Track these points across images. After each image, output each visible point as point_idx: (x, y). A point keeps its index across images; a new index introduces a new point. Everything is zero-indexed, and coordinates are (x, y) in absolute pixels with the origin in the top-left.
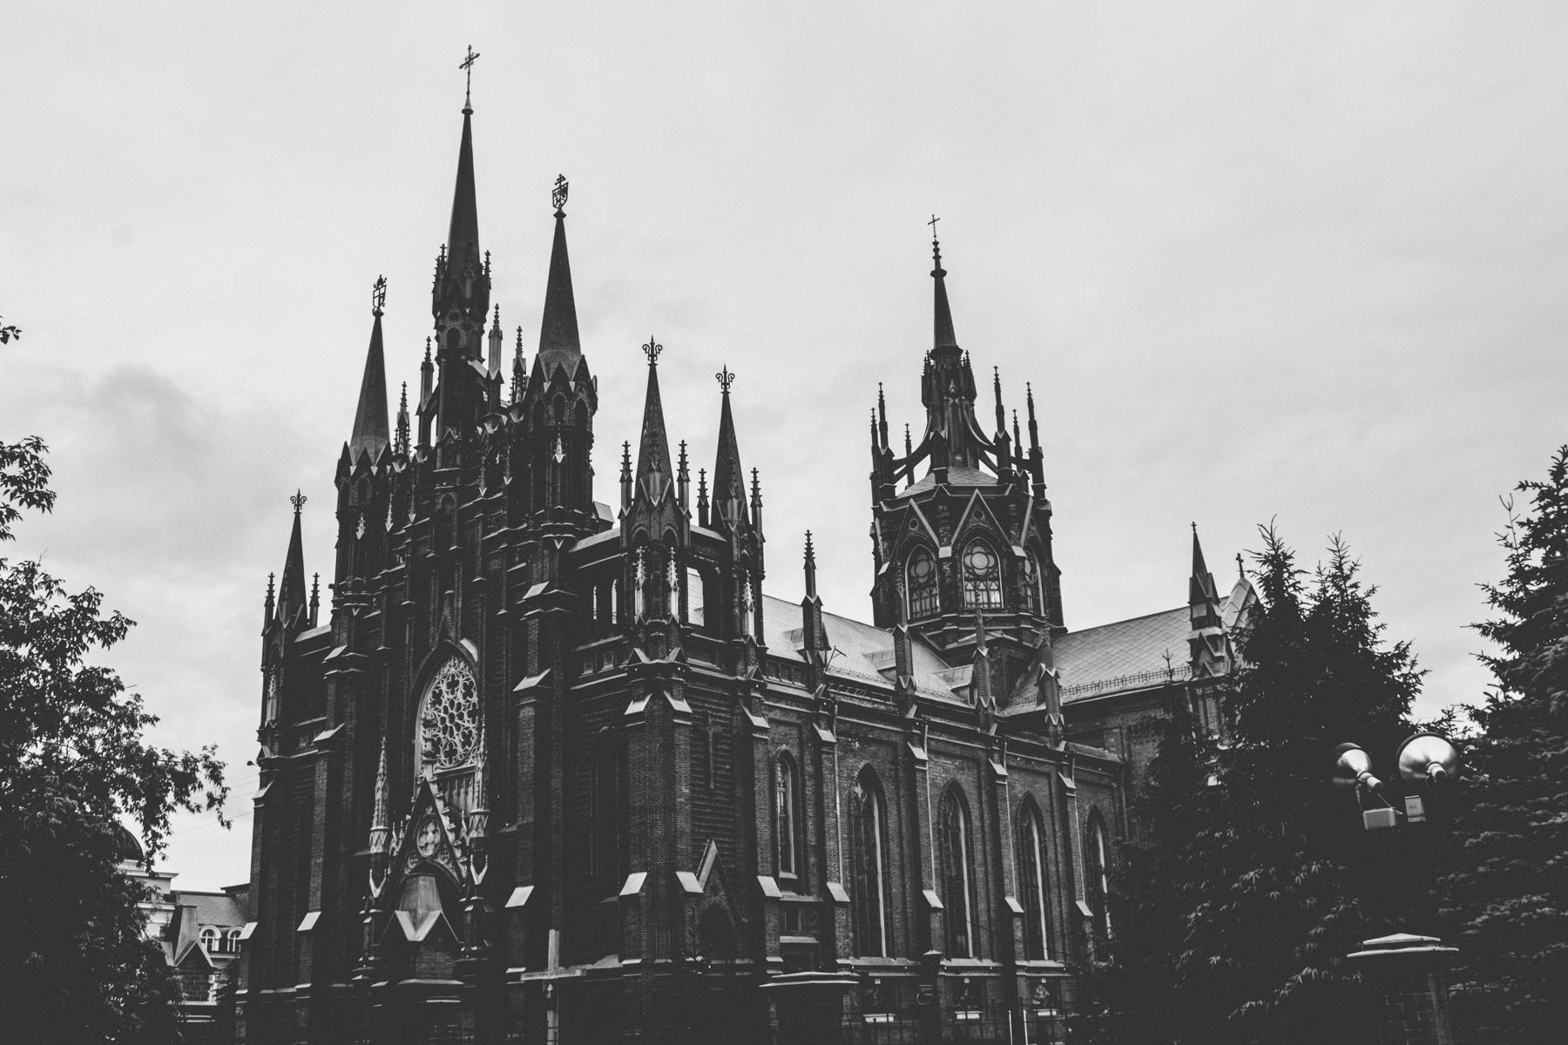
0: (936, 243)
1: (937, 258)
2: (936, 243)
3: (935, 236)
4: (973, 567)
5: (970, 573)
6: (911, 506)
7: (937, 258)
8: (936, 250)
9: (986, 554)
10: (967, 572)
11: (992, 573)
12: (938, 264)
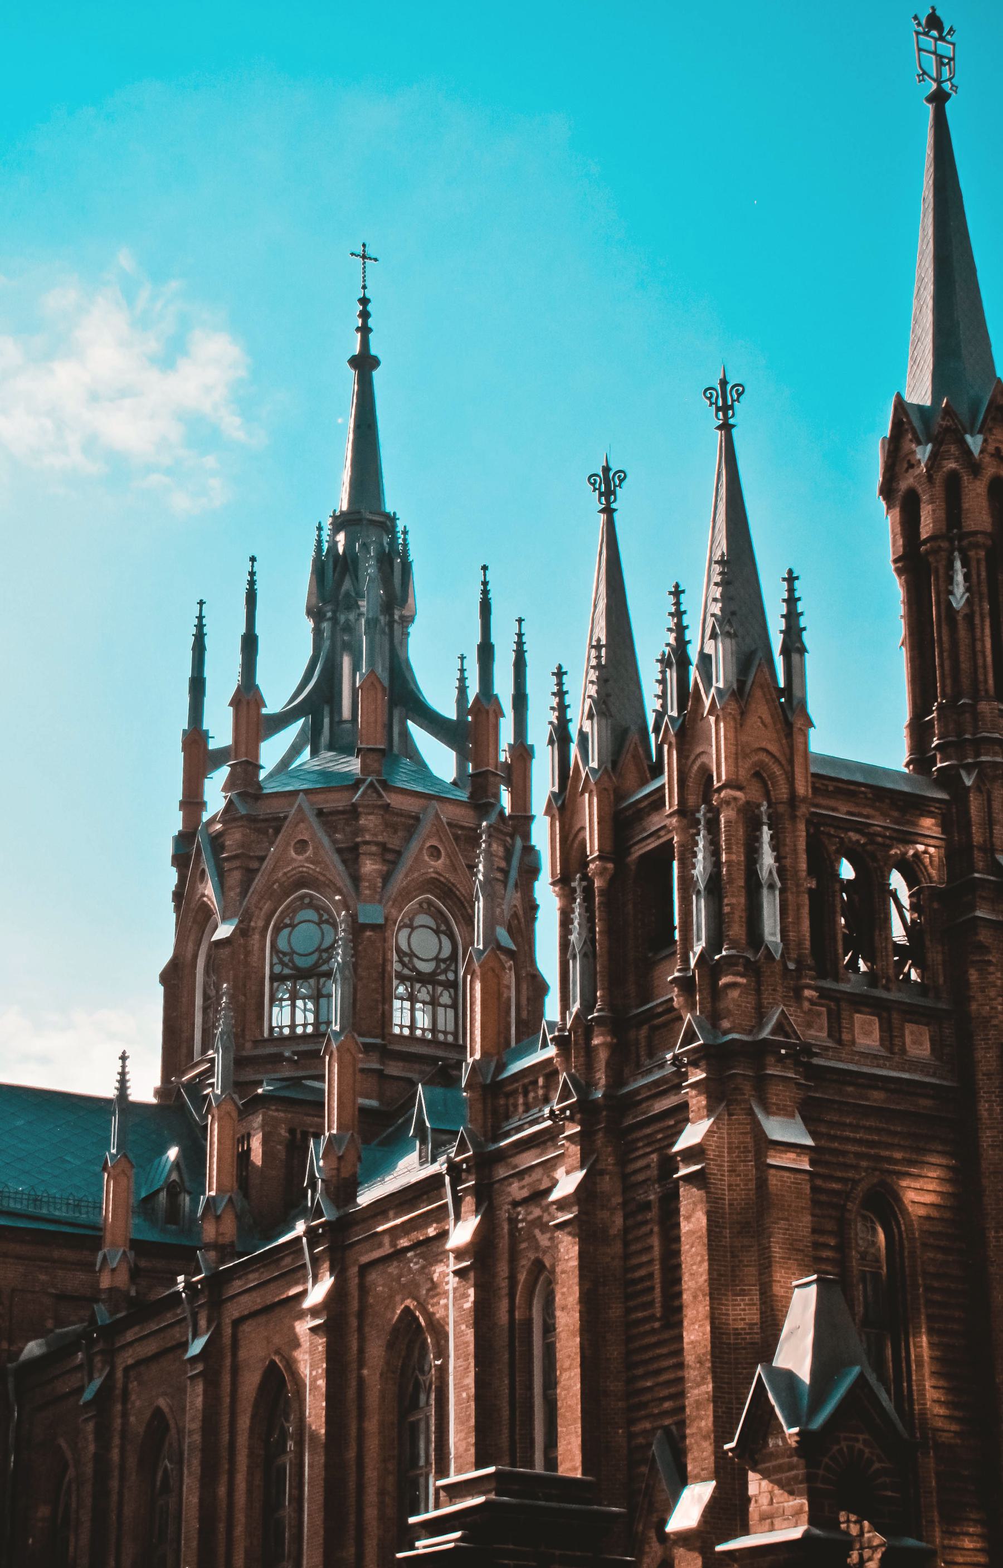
0: (364, 301)
1: (365, 330)
2: (364, 301)
3: (364, 287)
4: (412, 955)
5: (404, 965)
6: (300, 809)
7: (365, 330)
8: (365, 315)
9: (437, 932)
10: (401, 961)
11: (445, 971)
12: (365, 343)
